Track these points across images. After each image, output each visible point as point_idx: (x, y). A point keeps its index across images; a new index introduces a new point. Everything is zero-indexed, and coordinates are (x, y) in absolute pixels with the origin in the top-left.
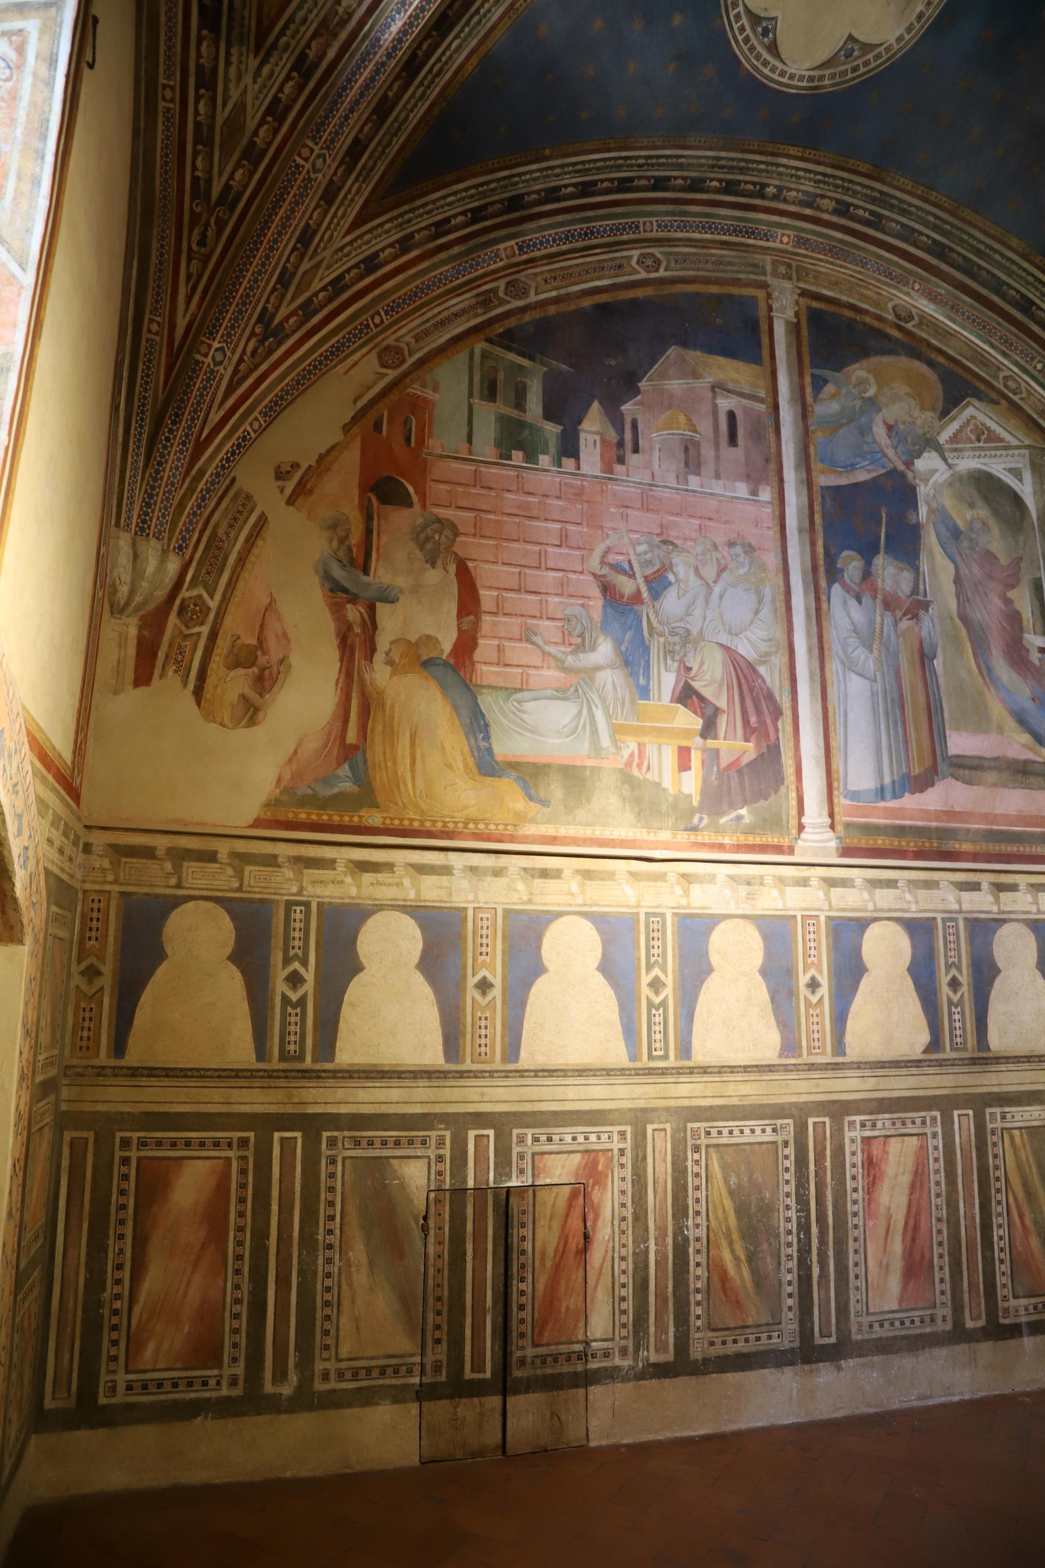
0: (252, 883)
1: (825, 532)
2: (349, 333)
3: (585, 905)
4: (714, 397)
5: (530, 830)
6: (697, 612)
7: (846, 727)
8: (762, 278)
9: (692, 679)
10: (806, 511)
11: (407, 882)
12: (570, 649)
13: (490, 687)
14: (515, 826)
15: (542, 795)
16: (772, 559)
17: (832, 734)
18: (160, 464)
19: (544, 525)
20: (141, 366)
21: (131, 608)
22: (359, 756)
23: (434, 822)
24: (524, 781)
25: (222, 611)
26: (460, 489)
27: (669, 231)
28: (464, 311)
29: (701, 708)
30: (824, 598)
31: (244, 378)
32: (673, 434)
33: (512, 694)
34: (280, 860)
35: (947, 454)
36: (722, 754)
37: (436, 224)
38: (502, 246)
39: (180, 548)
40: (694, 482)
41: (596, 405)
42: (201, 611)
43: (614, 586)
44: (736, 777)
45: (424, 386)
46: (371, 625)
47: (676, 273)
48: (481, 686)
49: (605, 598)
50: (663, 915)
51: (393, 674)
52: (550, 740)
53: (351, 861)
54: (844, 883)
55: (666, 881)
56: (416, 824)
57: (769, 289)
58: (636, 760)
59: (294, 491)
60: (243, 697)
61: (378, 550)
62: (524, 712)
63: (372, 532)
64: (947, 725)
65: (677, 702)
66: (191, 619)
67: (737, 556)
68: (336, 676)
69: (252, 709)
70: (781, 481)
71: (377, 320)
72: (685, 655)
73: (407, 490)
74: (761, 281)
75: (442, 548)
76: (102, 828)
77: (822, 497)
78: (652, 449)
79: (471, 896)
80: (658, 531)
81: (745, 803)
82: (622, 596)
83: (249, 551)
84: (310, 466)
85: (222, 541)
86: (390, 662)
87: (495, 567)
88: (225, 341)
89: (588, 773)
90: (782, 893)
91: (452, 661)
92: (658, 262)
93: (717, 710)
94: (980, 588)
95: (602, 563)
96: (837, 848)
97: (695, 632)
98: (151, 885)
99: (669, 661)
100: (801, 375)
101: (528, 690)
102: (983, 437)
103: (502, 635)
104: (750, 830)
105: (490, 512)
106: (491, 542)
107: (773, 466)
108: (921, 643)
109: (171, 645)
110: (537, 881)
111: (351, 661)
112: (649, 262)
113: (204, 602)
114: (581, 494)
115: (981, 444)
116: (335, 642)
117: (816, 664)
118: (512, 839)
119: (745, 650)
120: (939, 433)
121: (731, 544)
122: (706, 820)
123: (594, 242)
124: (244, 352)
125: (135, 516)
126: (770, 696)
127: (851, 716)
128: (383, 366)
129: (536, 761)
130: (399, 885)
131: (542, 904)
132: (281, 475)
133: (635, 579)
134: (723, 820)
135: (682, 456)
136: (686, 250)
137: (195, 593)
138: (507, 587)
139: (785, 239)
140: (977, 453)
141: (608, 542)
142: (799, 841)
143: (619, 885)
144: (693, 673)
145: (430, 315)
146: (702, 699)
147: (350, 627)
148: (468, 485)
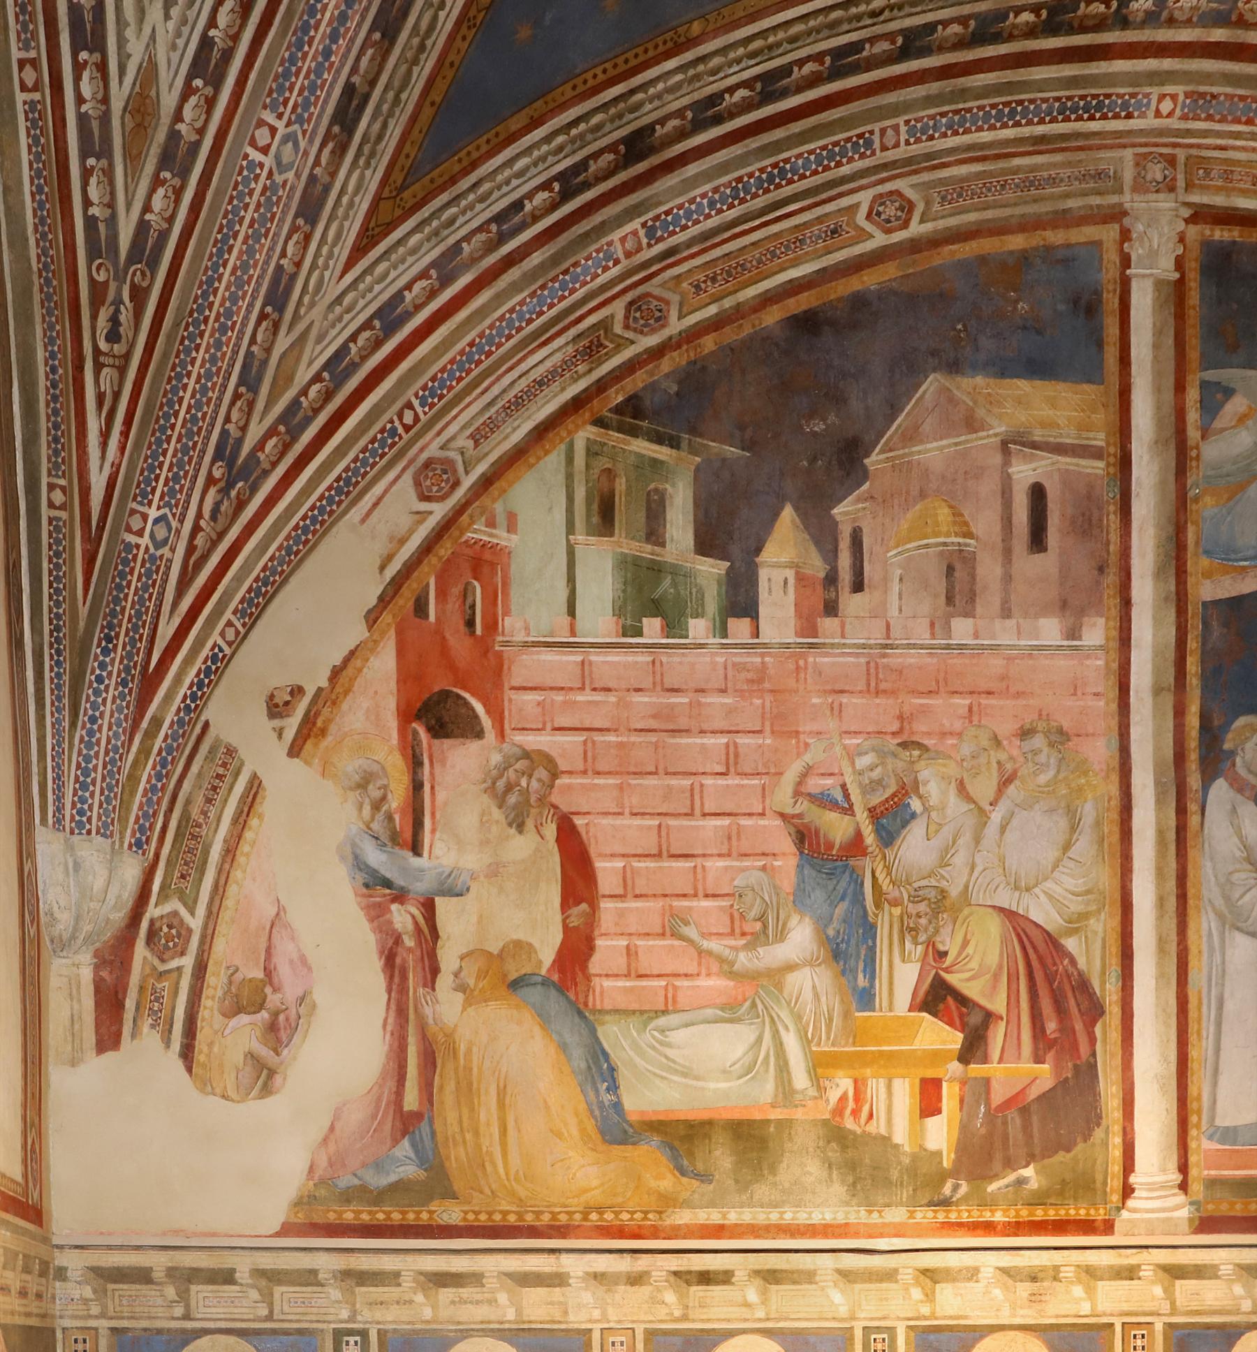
0: (286, 1309)
1: (1204, 688)
2: (364, 451)
3: (768, 1319)
4: (1007, 463)
5: (683, 1217)
6: (960, 859)
7: (1219, 1024)
8: (1114, 199)
9: (947, 970)
10: (1171, 654)
11: (503, 1298)
13: (616, 1011)
14: (660, 1213)
15: (700, 1166)
16: (1101, 751)
17: (1193, 1038)
18: (93, 720)
19: (698, 741)
20: (45, 565)
21: (79, 941)
23: (538, 1214)
24: (672, 1148)
25: (210, 932)
26: (559, 697)
27: (931, 138)
28: (553, 375)
29: (961, 1016)
30: (1193, 807)
31: (205, 558)
32: (927, 546)
33: (651, 1019)
34: (320, 1276)
36: (994, 1084)
37: (499, 218)
38: (616, 236)
39: (139, 844)
40: (962, 629)
41: (788, 513)
43: (817, 832)
44: (1018, 1121)
45: (491, 524)
46: (429, 931)
47: (941, 224)
49: (801, 853)
50: (891, 1331)
51: (468, 1003)
52: (712, 1085)
53: (421, 1273)
54: (1199, 1272)
55: (897, 1282)
56: (512, 1219)
57: (1126, 221)
58: (851, 1104)
60: (251, 1055)
61: (433, 814)
62: (669, 1045)
65: (920, 1010)
66: (167, 948)
67: (1036, 752)
68: (383, 1014)
69: (265, 1072)
70: (1126, 603)
71: (408, 418)
72: (937, 931)
73: (473, 710)
74: (1114, 206)
76: (77, 1247)
77: (1206, 624)
78: (886, 580)
79: (596, 1314)
80: (895, 727)
81: (1031, 1158)
82: (830, 846)
83: (240, 837)
84: (320, 690)
85: (199, 826)
86: (462, 988)
87: (618, 821)
88: (168, 505)
89: (772, 1129)
90: (1090, 1291)
91: (556, 977)
92: (908, 207)
93: (989, 1017)
95: (797, 793)
96: (1191, 1220)
97: (954, 891)
98: (150, 1318)
99: (908, 945)
100: (1180, 387)
103: (633, 930)
104: (1038, 1199)
105: (608, 730)
106: (611, 781)
107: (1111, 578)
109: (142, 989)
110: (693, 1288)
111: (403, 990)
112: (890, 210)
114: (760, 681)
116: (377, 964)
117: (1171, 924)
118: (655, 1233)
119: (1042, 912)
121: (1025, 733)
122: (964, 1188)
123: (788, 191)
124: (199, 515)
125: (68, 806)
126: (1083, 986)
127: (1229, 1006)
128: (424, 498)
129: (689, 1118)
130: (492, 1302)
131: (702, 1321)
132: (276, 709)
133: (853, 814)
134: (992, 1187)
135: (941, 587)
136: (964, 170)
137: (167, 908)
138: (639, 851)
139: (1166, 106)
141: (808, 758)
142: (1125, 1214)
143: (823, 1289)
144: (949, 960)
145: (496, 390)
146: (962, 1000)
147: (398, 940)
148: (571, 689)
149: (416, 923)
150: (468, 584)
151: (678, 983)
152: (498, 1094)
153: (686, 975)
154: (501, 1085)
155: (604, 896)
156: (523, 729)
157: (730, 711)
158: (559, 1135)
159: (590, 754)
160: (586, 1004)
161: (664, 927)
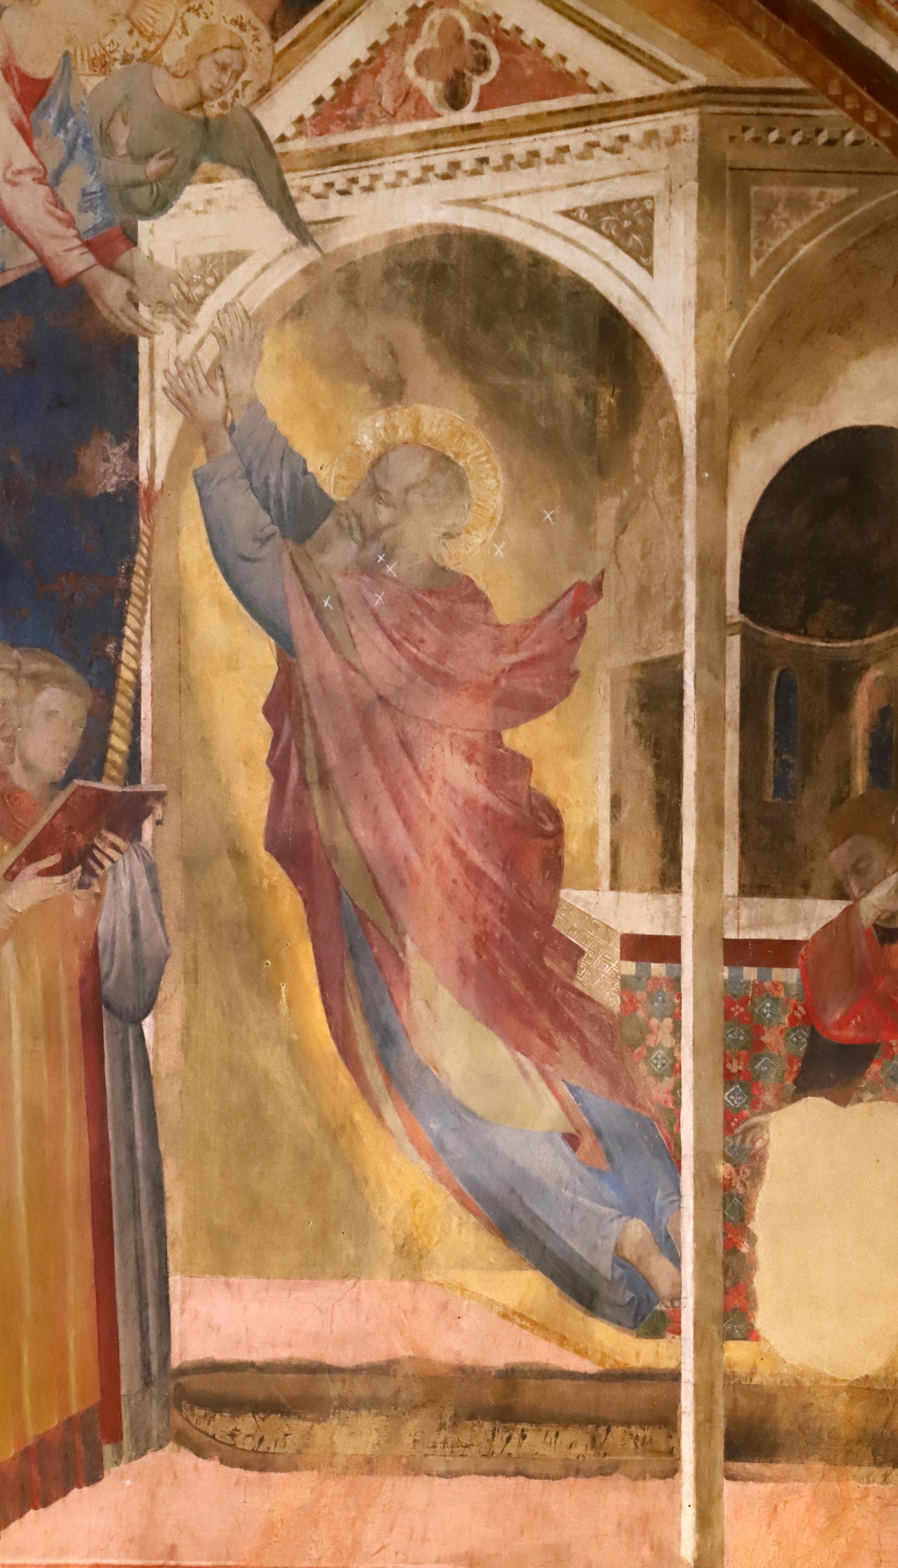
35: (293, 180)
64: (175, 1256)
94: (384, 723)
102: (478, 83)
108: (93, 958)
115: (467, 116)
120: (265, 91)
140: (440, 160)
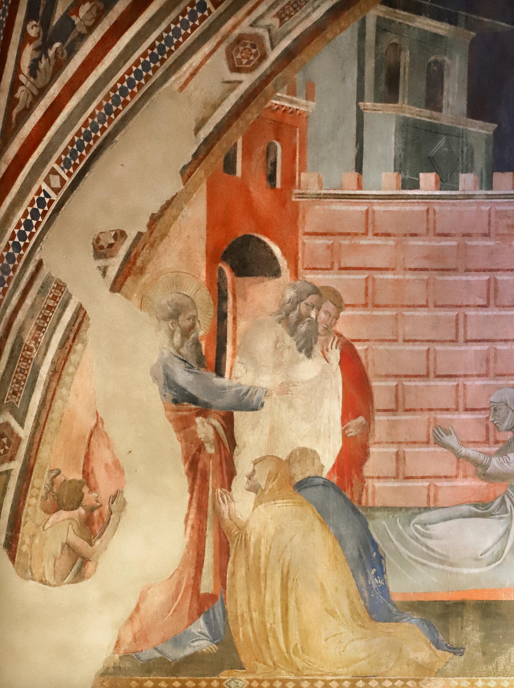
12: (495, 449)
13: (386, 508)
14: (417, 681)
15: (453, 641)
19: (464, 278)
22: (218, 606)
24: (430, 625)
25: (37, 440)
26: (346, 242)
33: (415, 515)
42: (9, 443)
45: (292, 92)
48: (374, 509)
51: (258, 502)
52: (465, 571)
59: (120, 270)
60: (68, 546)
61: (234, 341)
62: (430, 537)
63: (225, 316)
69: (79, 560)
73: (271, 252)
75: (320, 329)
83: (66, 360)
84: (140, 234)
85: (30, 350)
86: (254, 489)
87: (394, 347)
91: (335, 479)
101: (436, 508)
103: (402, 440)
105: (387, 269)
106: (388, 313)
111: (204, 490)
113: (12, 432)
116: (183, 468)
128: (235, 69)
129: (445, 599)
138: (410, 373)
147: (201, 448)
148: (356, 234)
149: (217, 434)
150: (271, 144)
151: (439, 483)
152: (282, 579)
153: (446, 477)
154: (285, 570)
155: (378, 410)
156: (315, 269)
157: (491, 252)
158: (332, 613)
159: (370, 291)
160: (360, 502)
161: (428, 436)
